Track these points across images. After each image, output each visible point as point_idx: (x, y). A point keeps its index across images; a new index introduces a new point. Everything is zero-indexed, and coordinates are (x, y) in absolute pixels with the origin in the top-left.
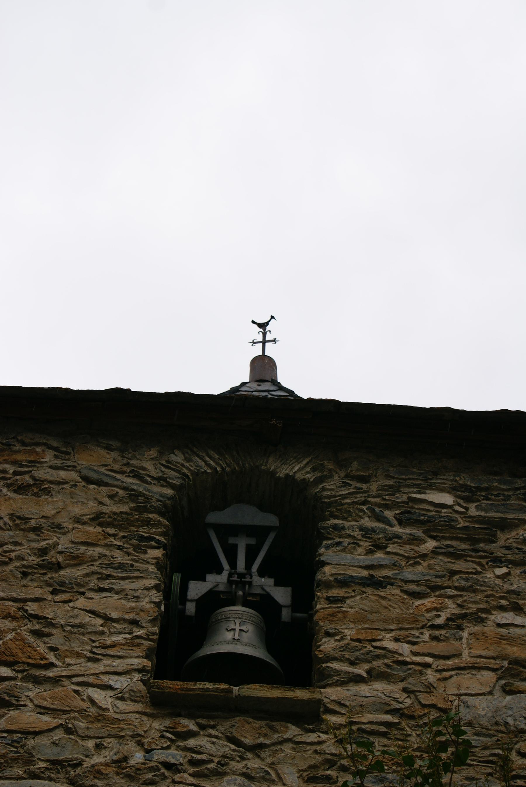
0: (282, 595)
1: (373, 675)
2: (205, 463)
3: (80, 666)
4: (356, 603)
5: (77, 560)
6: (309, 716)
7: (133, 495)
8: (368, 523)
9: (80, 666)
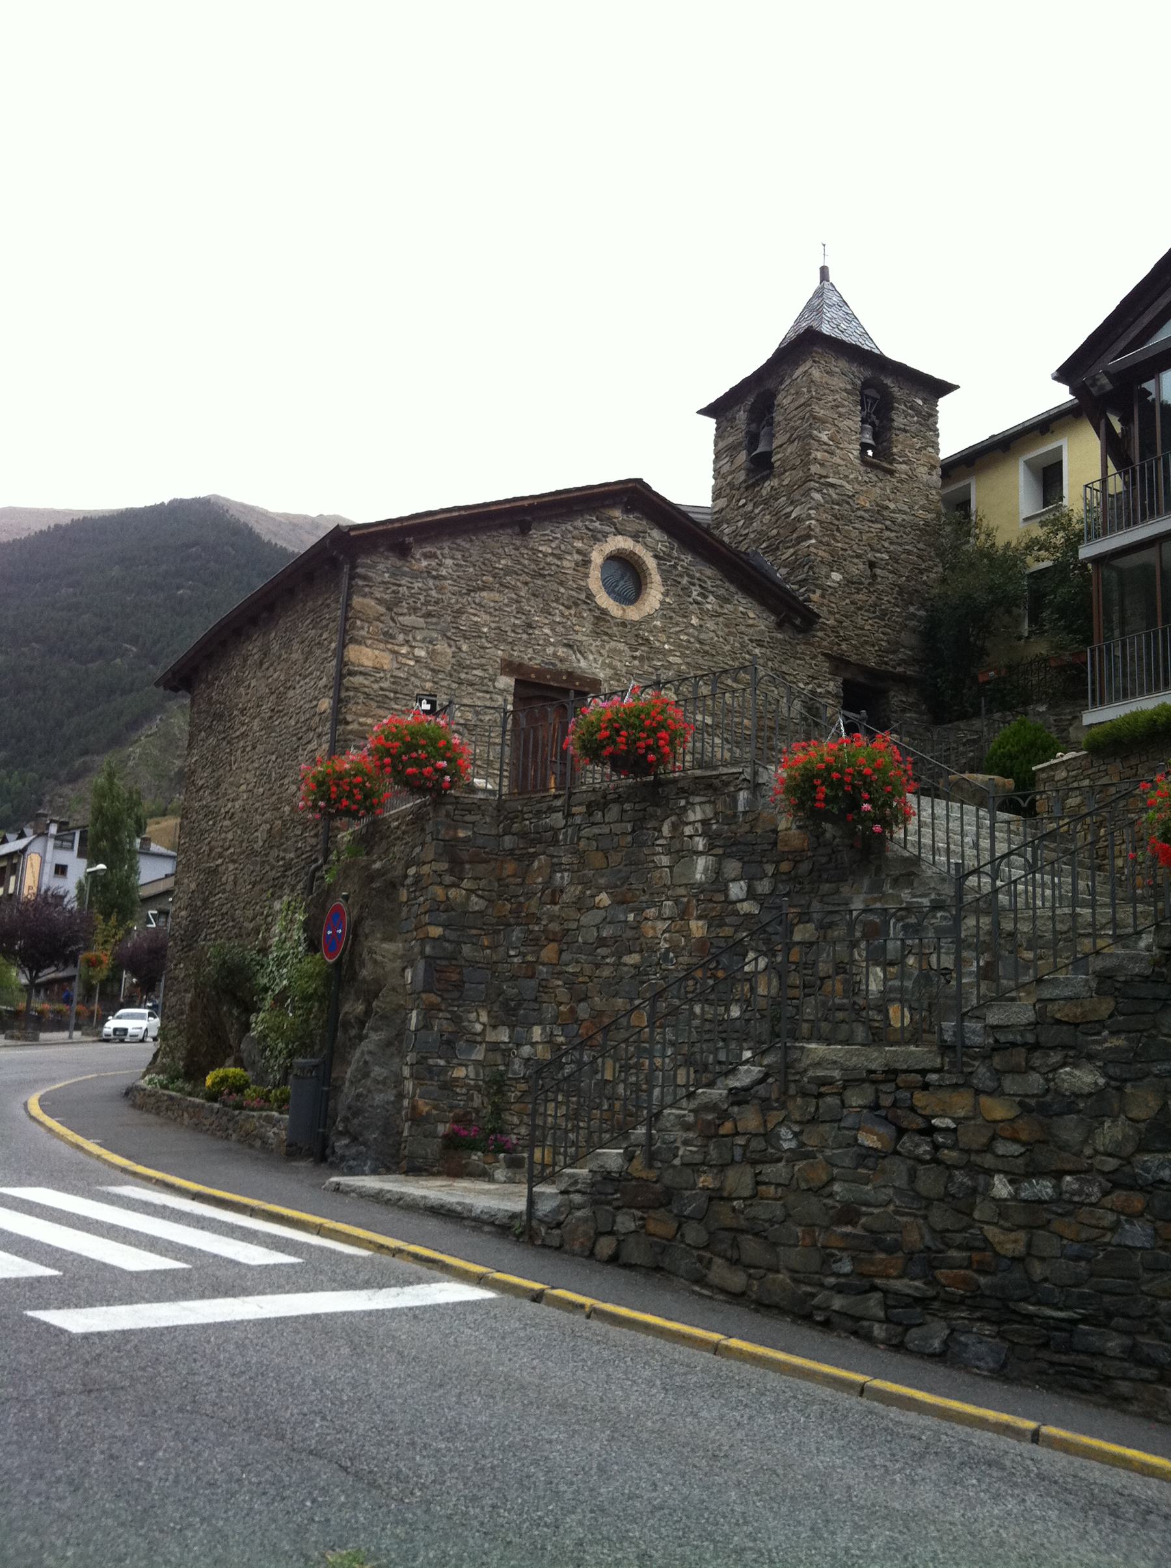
0: (877, 422)
1: (904, 462)
2: (868, 374)
3: (846, 445)
4: (902, 436)
5: (843, 406)
6: (891, 472)
7: (853, 384)
8: (903, 407)
9: (846, 445)
